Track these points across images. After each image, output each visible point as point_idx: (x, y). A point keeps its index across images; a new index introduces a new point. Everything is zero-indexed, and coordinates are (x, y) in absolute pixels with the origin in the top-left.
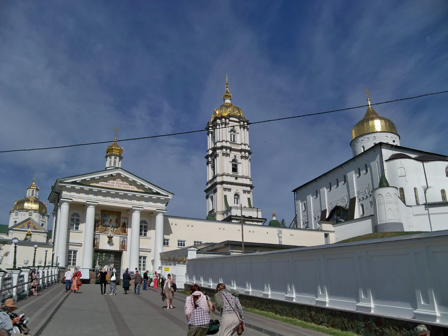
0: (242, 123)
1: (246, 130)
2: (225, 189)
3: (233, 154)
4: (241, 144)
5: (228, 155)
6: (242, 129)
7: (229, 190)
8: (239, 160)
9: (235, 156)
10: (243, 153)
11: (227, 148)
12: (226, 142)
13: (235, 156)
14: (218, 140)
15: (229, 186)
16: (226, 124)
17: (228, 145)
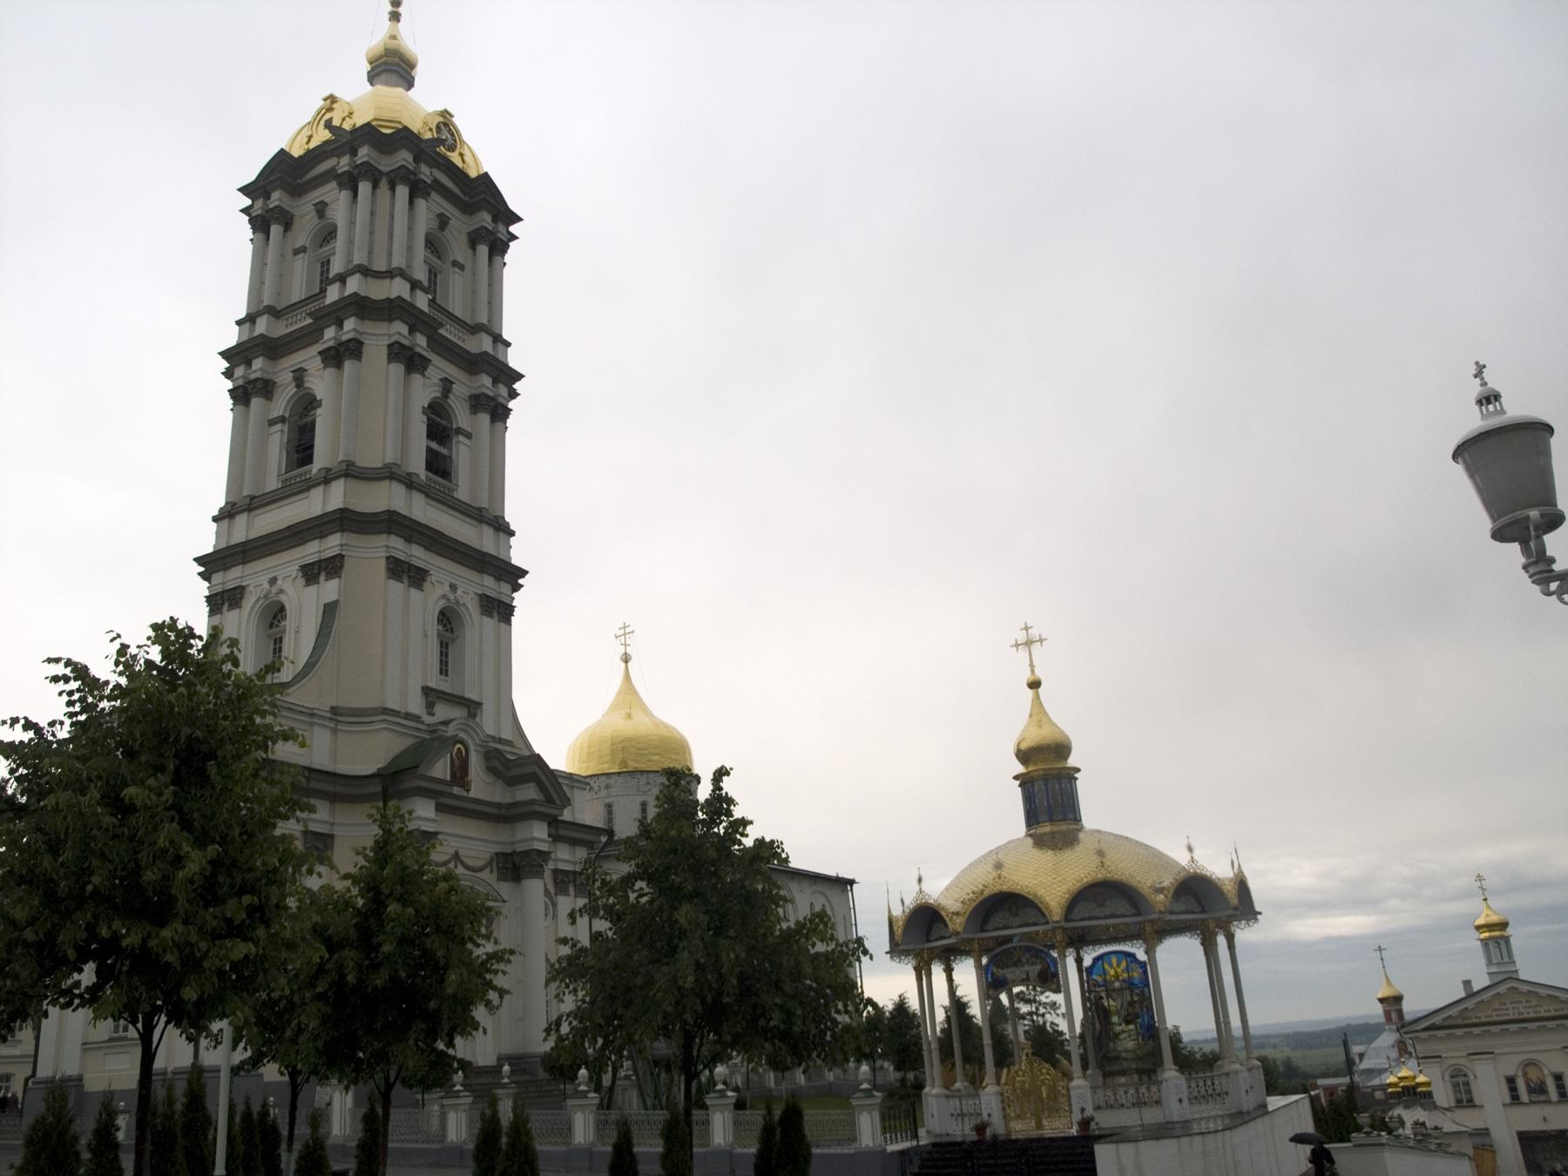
0: (485, 219)
1: (497, 259)
2: (399, 569)
3: (440, 367)
4: (476, 329)
5: (412, 362)
6: (483, 250)
7: (415, 576)
8: (462, 417)
9: (447, 385)
10: (486, 380)
11: (416, 320)
12: (415, 285)
13: (447, 385)
14: (359, 258)
15: (418, 555)
16: (418, 190)
17: (422, 301)
